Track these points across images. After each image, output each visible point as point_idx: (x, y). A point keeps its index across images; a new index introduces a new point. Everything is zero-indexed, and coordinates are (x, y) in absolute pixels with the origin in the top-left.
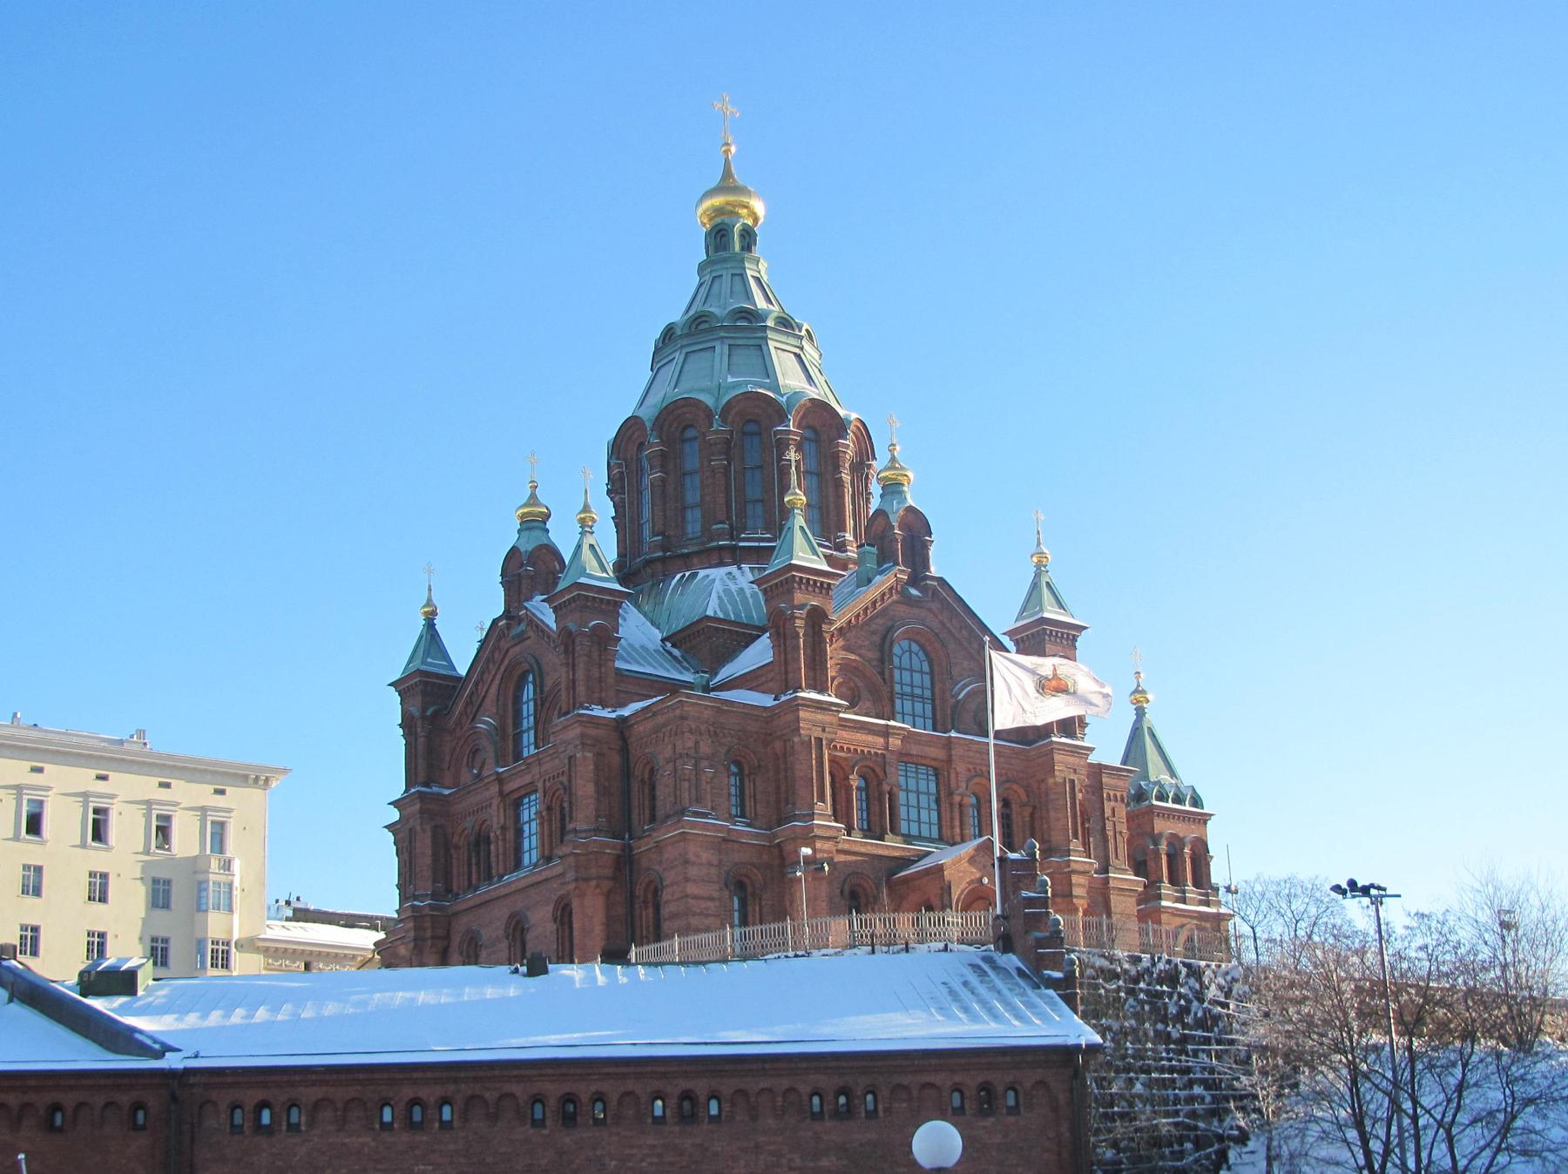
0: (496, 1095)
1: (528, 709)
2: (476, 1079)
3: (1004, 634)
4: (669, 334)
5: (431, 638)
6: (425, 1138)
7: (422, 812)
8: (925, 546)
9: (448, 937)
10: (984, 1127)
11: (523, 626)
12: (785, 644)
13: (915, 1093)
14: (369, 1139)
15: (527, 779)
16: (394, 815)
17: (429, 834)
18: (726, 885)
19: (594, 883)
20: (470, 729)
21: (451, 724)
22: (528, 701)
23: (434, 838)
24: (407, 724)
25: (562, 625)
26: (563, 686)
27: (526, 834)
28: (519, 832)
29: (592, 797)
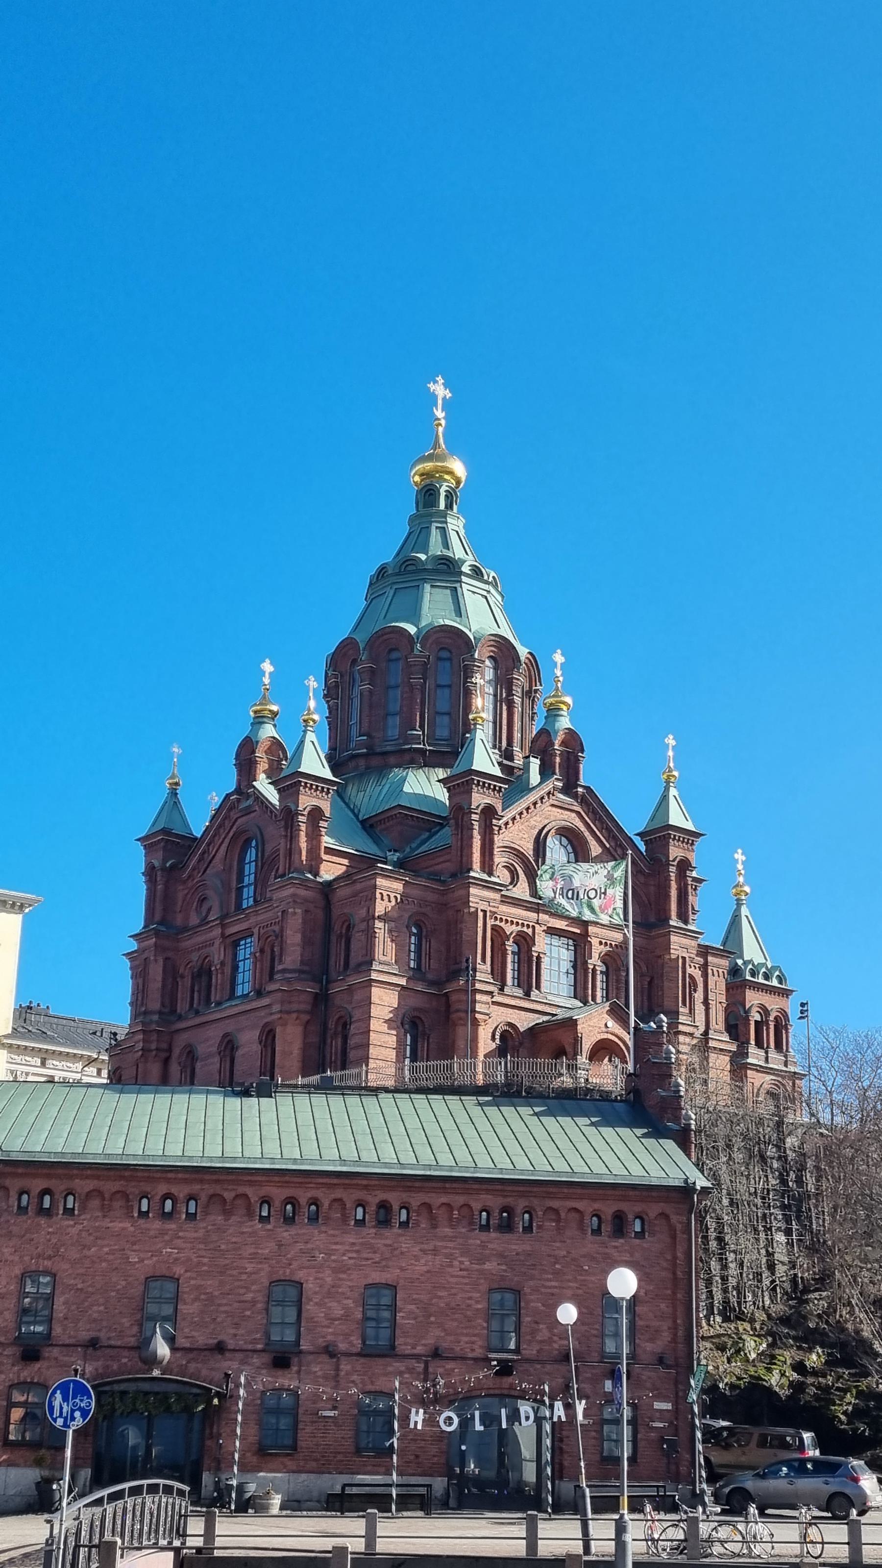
0: (233, 1194)
1: (250, 869)
2: (217, 1181)
3: (637, 835)
4: (382, 572)
8: (577, 761)
9: (170, 1050)
10: (616, 1247)
11: (250, 802)
12: (462, 832)
13: (563, 1215)
16: (133, 946)
18: (402, 1024)
19: (294, 1015)
20: (200, 881)
22: (250, 862)
24: (150, 873)
26: (282, 852)
27: (241, 970)
28: (235, 968)
29: (298, 945)
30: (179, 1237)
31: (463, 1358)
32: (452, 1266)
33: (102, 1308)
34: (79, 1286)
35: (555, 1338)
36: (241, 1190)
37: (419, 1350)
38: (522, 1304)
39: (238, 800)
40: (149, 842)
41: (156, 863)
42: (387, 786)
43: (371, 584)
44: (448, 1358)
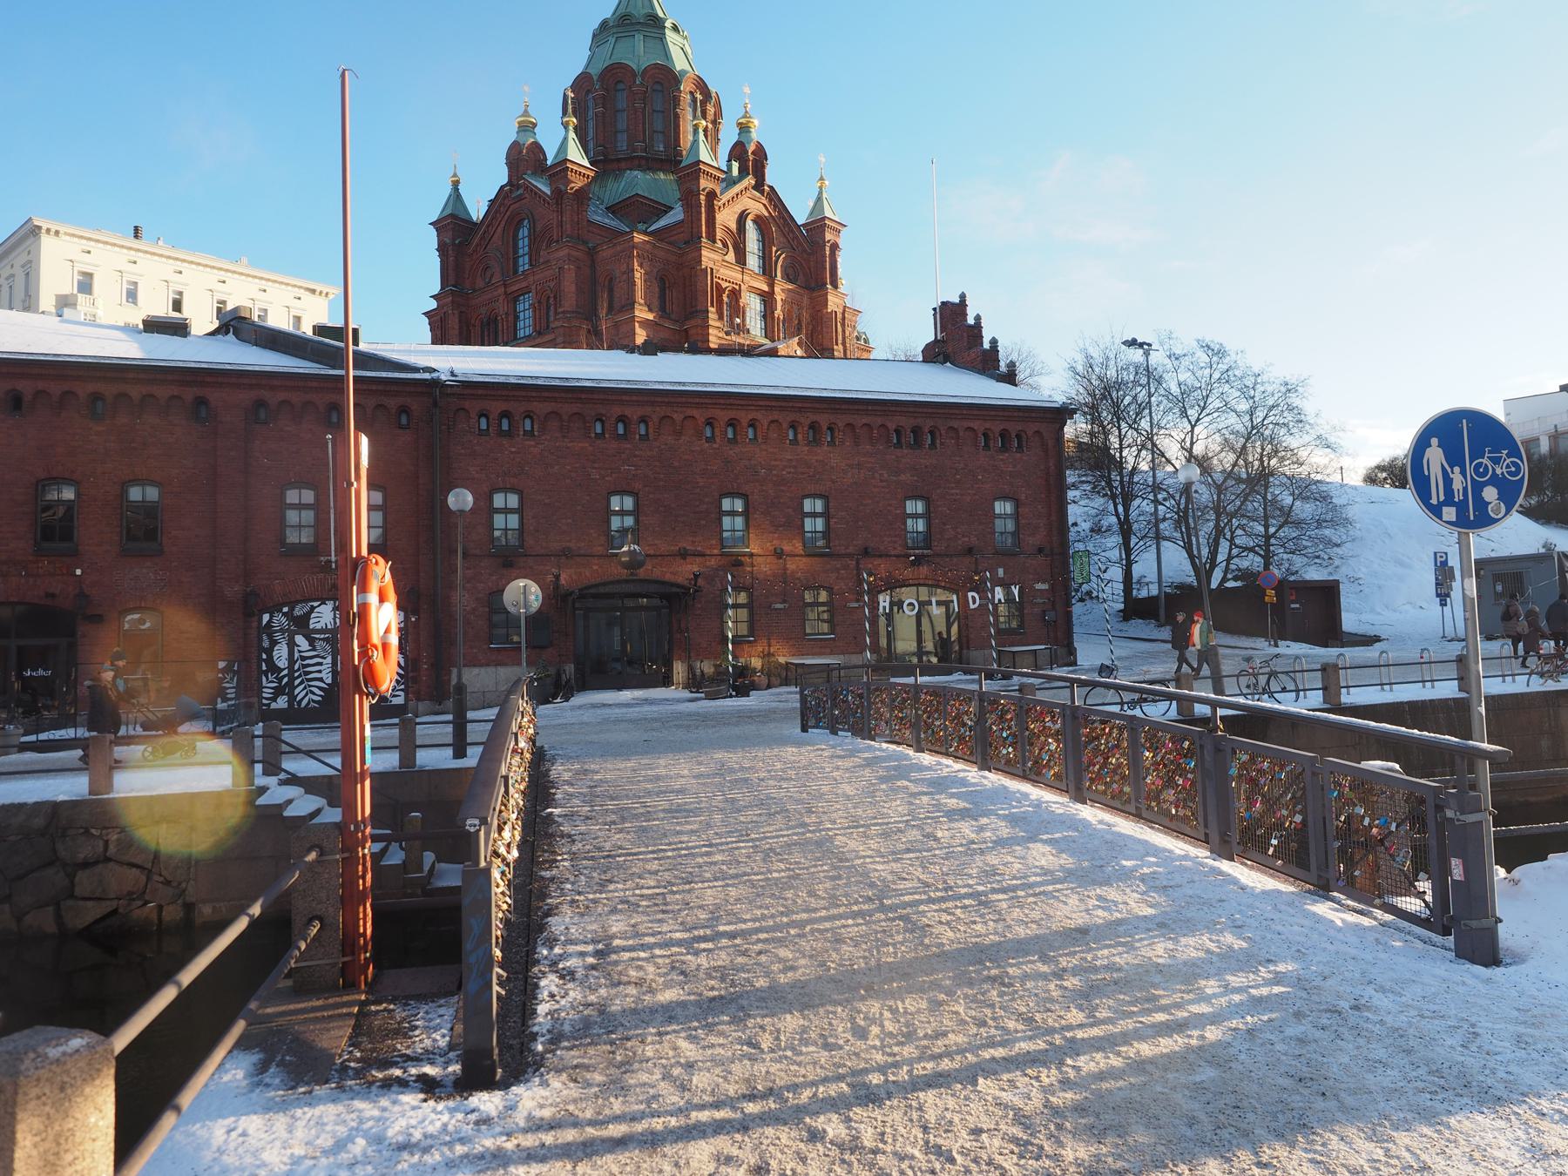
1: (524, 245)
2: (668, 404)
4: (604, 25)
5: (456, 196)
6: (629, 446)
7: (453, 302)
8: (763, 167)
10: (1002, 460)
11: (520, 191)
13: (961, 434)
14: (587, 445)
15: (524, 284)
17: (457, 316)
21: (470, 251)
22: (523, 238)
23: (460, 316)
24: (442, 249)
25: (554, 187)
30: (636, 456)
31: (887, 556)
32: (874, 478)
33: (570, 521)
34: (547, 501)
35: (959, 536)
36: (690, 412)
37: (851, 550)
38: (932, 509)
39: (511, 191)
40: (438, 225)
41: (447, 241)
42: (623, 183)
43: (594, 36)
44: (875, 556)
